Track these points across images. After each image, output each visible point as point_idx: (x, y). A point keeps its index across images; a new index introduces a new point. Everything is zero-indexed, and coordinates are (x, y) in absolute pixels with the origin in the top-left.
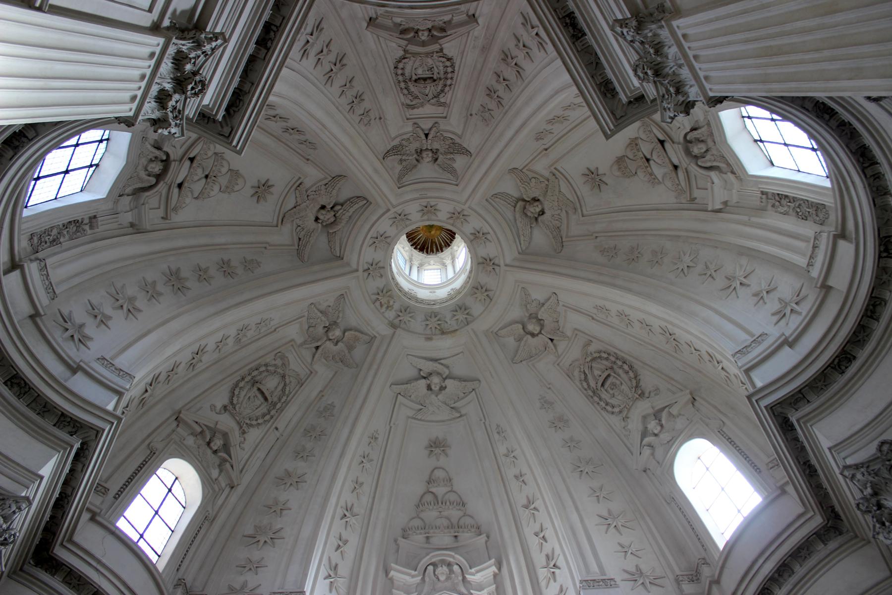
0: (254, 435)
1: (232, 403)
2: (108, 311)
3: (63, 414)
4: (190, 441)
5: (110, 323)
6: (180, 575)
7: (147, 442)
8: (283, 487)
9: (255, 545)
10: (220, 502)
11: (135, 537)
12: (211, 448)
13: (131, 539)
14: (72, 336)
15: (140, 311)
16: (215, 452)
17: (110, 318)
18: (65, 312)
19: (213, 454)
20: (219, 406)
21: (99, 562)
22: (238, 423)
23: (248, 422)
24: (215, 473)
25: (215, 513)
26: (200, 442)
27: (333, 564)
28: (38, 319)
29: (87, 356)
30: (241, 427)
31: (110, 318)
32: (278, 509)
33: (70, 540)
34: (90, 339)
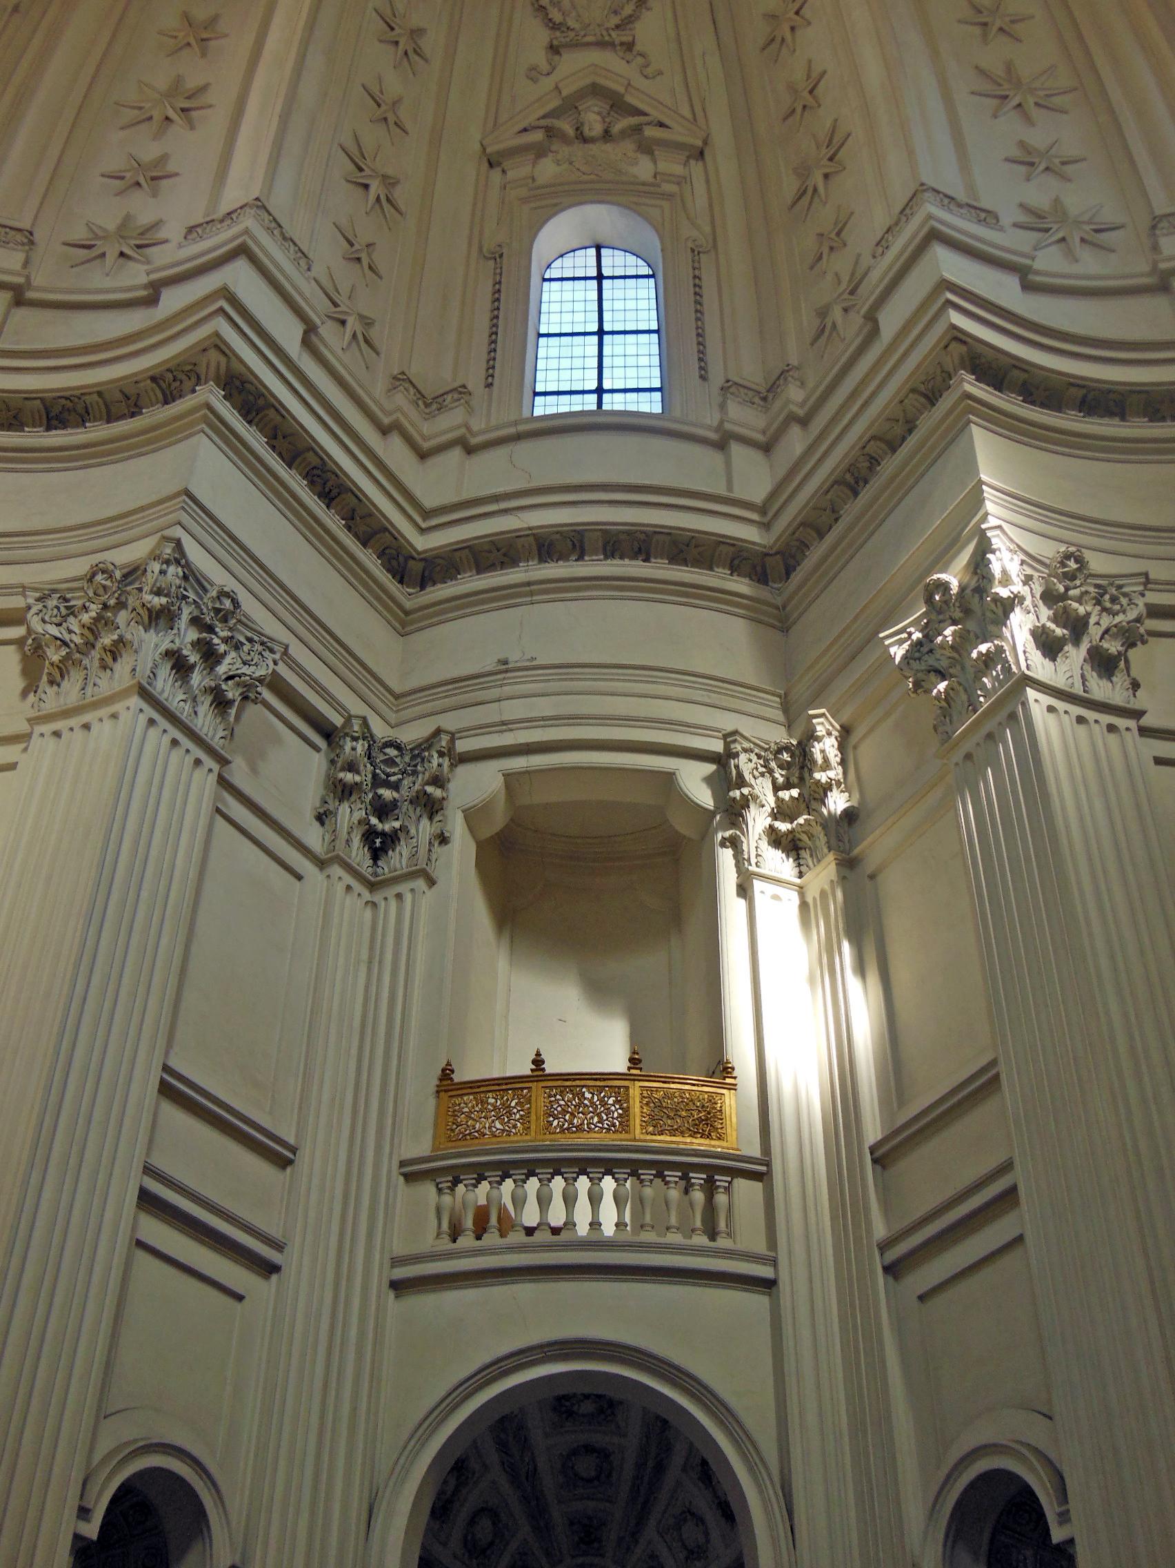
0: (651, 30)
1: (554, 26)
2: (149, 151)
3: (153, 379)
4: (547, 169)
5: (171, 167)
6: (717, 376)
7: (474, 254)
8: (784, 50)
9: (816, 199)
10: (701, 201)
11: (590, 402)
12: (591, 140)
13: (582, 413)
14: (122, 254)
15: (204, 89)
16: (607, 135)
17: (164, 158)
18: (80, 234)
19: (582, 143)
20: (540, 58)
21: (496, 498)
22: (601, 44)
23: (615, 20)
24: (643, 169)
25: (708, 229)
26: (564, 151)
27: (1000, 72)
28: (31, 295)
29: (172, 253)
30: (611, 45)
31: (164, 158)
32: (806, 97)
33: (427, 514)
34: (157, 225)
